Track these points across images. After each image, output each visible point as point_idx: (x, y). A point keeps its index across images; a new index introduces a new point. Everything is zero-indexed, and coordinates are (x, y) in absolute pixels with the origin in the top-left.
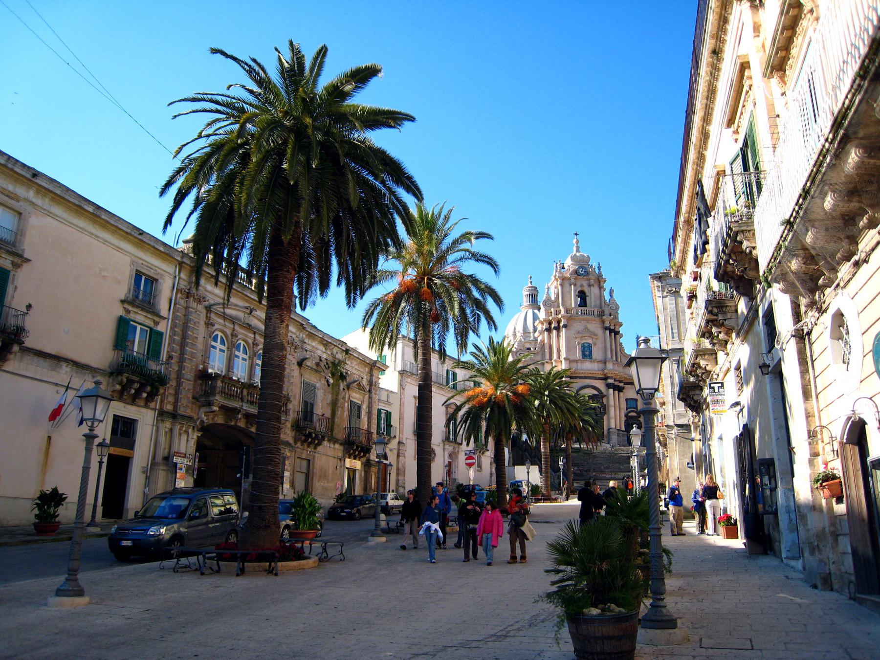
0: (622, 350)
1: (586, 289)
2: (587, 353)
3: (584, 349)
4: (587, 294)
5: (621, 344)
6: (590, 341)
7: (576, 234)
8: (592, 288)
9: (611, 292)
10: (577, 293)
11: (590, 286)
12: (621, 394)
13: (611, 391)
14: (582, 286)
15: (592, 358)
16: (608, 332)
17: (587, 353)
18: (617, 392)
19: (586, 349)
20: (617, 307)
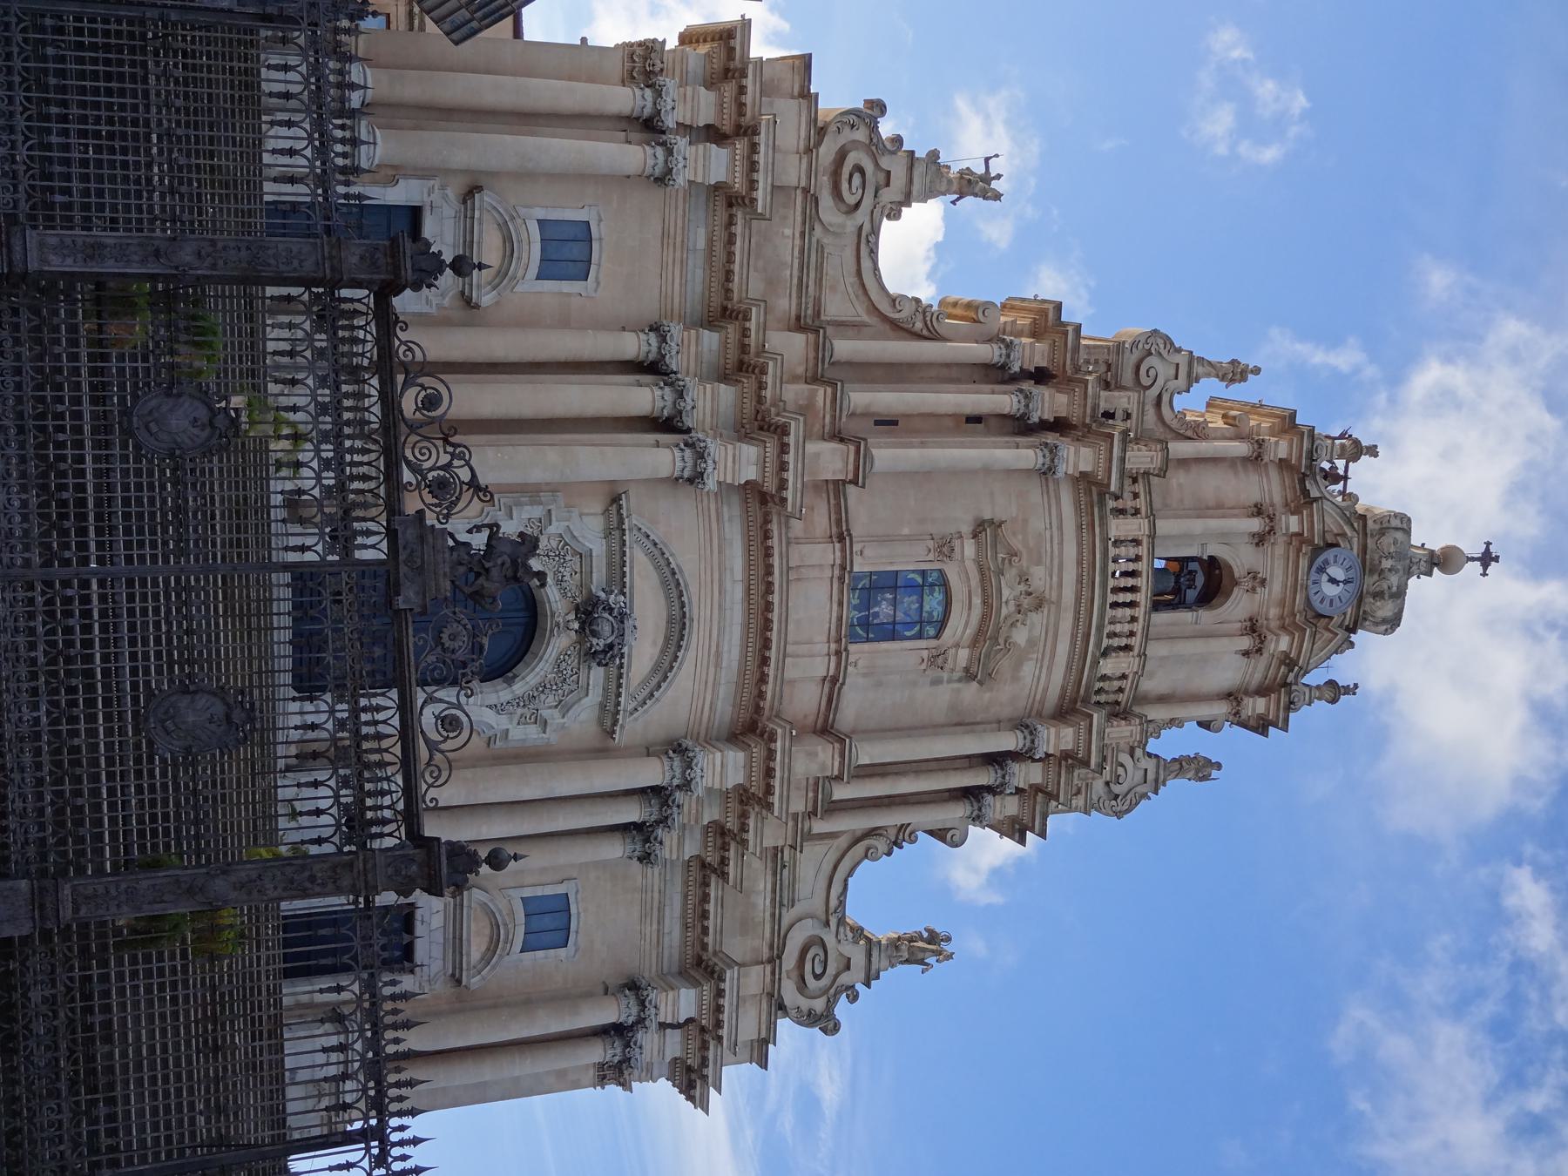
0: (868, 843)
1: (1238, 606)
2: (884, 610)
3: (911, 586)
4: (1206, 616)
5: (902, 837)
6: (961, 625)
7: (1487, 559)
8: (1246, 643)
9: (1201, 768)
10: (1214, 550)
11: (1253, 627)
12: (614, 850)
13: (652, 773)
14: (1258, 581)
15: (854, 638)
16: (1008, 742)
17: (884, 610)
18: (631, 813)
19: (909, 602)
20: (1119, 803)
